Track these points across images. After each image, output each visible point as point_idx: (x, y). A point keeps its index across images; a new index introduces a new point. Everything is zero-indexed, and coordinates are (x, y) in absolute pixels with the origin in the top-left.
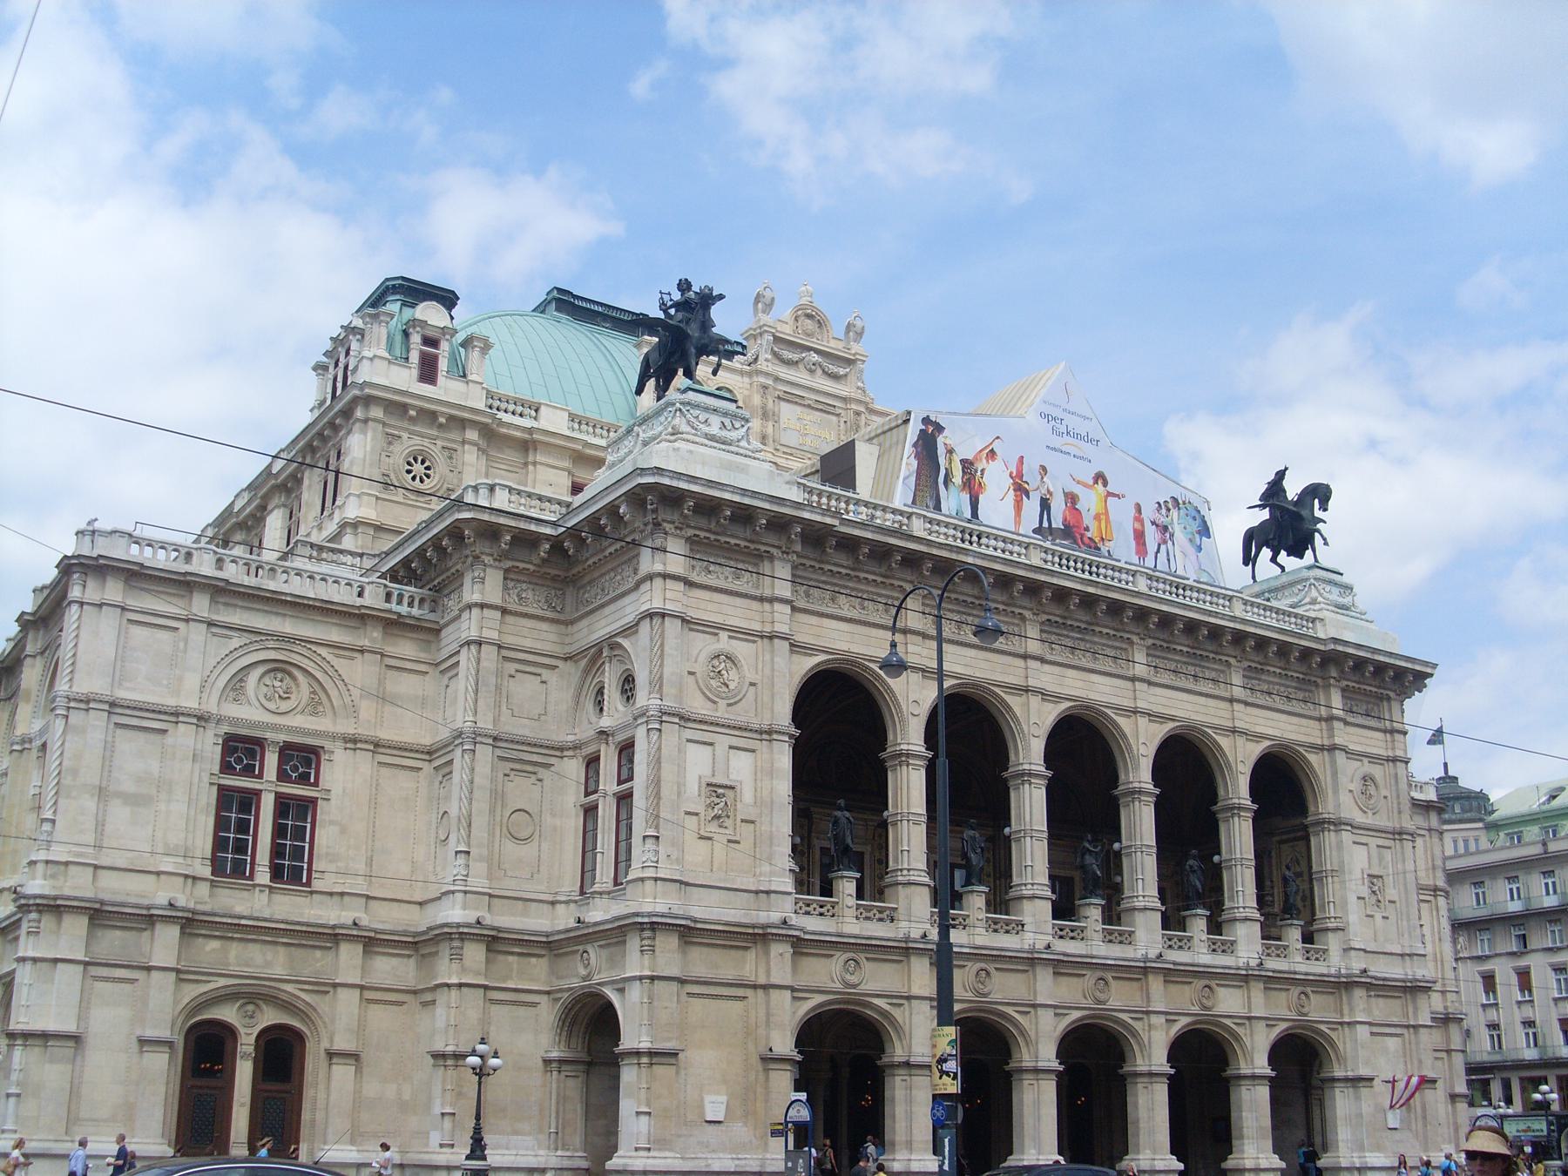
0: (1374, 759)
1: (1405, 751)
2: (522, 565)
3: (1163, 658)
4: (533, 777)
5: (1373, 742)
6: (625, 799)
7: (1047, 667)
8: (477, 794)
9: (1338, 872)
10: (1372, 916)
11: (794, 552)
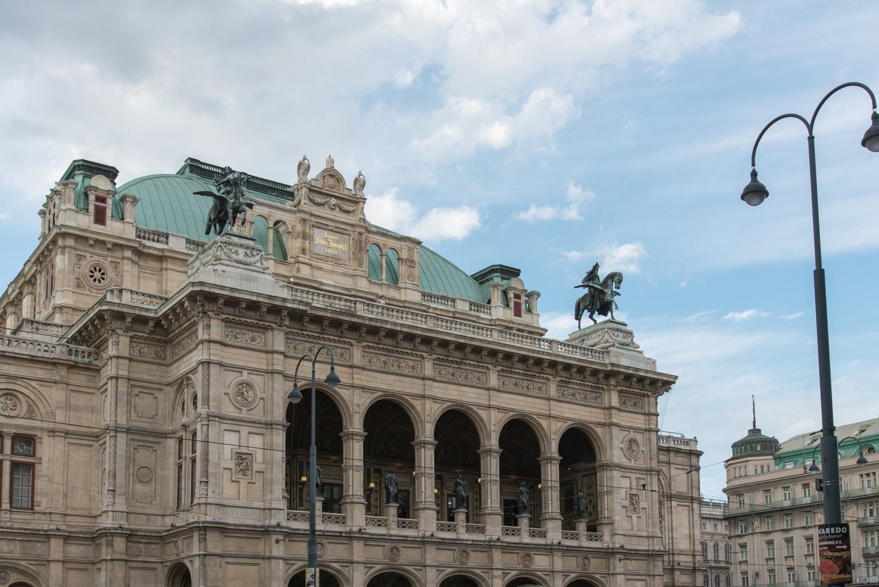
0: (637, 430)
1: (657, 425)
2: (140, 334)
3: (508, 377)
4: (151, 449)
5: (638, 421)
6: (194, 461)
7: (435, 384)
8: (118, 460)
10: (631, 517)
11: (284, 325)
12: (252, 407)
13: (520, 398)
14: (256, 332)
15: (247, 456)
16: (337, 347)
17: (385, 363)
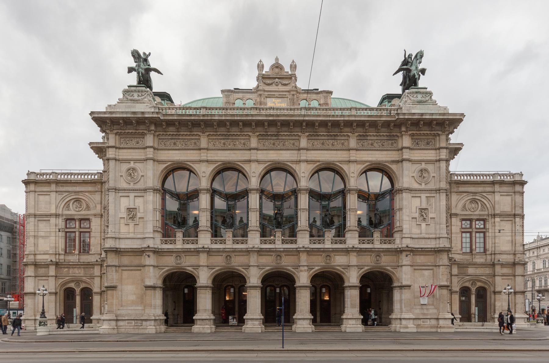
0: (428, 162)
3: (317, 139)
5: (431, 155)
7: (259, 152)
9: (401, 209)
12: (137, 181)
13: (326, 152)
14: (139, 138)
15: (133, 210)
16: (191, 139)
17: (224, 144)
